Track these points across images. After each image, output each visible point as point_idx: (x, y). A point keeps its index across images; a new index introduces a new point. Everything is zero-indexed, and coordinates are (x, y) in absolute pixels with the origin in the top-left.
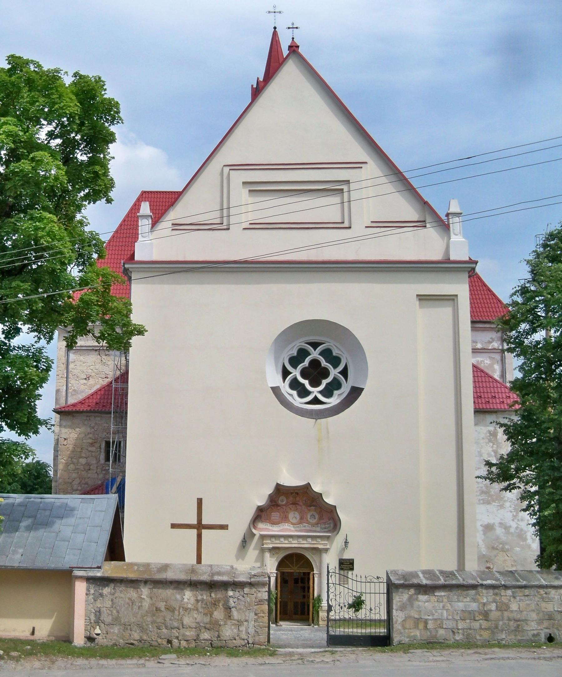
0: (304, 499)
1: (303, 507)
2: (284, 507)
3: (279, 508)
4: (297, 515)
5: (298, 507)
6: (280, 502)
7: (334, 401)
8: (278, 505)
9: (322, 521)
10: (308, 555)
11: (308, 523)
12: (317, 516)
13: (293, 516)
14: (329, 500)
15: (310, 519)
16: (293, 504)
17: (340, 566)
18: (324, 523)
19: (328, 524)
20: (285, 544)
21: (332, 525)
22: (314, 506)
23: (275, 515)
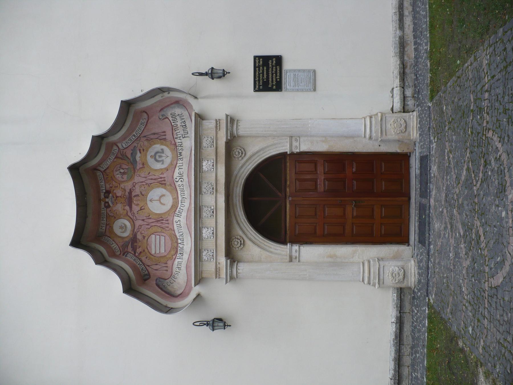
0: (118, 177)
1: (137, 179)
2: (138, 223)
3: (139, 237)
4: (156, 193)
5: (137, 191)
7: (244, 154)
8: (134, 240)
9: (169, 136)
10: (245, 168)
11: (173, 166)
12: (157, 147)
13: (158, 202)
14: (106, 118)
15: (163, 162)
17: (271, 90)
18: (173, 129)
19: (175, 120)
20: (215, 225)
21: (178, 111)
22: (134, 154)
23: (157, 245)
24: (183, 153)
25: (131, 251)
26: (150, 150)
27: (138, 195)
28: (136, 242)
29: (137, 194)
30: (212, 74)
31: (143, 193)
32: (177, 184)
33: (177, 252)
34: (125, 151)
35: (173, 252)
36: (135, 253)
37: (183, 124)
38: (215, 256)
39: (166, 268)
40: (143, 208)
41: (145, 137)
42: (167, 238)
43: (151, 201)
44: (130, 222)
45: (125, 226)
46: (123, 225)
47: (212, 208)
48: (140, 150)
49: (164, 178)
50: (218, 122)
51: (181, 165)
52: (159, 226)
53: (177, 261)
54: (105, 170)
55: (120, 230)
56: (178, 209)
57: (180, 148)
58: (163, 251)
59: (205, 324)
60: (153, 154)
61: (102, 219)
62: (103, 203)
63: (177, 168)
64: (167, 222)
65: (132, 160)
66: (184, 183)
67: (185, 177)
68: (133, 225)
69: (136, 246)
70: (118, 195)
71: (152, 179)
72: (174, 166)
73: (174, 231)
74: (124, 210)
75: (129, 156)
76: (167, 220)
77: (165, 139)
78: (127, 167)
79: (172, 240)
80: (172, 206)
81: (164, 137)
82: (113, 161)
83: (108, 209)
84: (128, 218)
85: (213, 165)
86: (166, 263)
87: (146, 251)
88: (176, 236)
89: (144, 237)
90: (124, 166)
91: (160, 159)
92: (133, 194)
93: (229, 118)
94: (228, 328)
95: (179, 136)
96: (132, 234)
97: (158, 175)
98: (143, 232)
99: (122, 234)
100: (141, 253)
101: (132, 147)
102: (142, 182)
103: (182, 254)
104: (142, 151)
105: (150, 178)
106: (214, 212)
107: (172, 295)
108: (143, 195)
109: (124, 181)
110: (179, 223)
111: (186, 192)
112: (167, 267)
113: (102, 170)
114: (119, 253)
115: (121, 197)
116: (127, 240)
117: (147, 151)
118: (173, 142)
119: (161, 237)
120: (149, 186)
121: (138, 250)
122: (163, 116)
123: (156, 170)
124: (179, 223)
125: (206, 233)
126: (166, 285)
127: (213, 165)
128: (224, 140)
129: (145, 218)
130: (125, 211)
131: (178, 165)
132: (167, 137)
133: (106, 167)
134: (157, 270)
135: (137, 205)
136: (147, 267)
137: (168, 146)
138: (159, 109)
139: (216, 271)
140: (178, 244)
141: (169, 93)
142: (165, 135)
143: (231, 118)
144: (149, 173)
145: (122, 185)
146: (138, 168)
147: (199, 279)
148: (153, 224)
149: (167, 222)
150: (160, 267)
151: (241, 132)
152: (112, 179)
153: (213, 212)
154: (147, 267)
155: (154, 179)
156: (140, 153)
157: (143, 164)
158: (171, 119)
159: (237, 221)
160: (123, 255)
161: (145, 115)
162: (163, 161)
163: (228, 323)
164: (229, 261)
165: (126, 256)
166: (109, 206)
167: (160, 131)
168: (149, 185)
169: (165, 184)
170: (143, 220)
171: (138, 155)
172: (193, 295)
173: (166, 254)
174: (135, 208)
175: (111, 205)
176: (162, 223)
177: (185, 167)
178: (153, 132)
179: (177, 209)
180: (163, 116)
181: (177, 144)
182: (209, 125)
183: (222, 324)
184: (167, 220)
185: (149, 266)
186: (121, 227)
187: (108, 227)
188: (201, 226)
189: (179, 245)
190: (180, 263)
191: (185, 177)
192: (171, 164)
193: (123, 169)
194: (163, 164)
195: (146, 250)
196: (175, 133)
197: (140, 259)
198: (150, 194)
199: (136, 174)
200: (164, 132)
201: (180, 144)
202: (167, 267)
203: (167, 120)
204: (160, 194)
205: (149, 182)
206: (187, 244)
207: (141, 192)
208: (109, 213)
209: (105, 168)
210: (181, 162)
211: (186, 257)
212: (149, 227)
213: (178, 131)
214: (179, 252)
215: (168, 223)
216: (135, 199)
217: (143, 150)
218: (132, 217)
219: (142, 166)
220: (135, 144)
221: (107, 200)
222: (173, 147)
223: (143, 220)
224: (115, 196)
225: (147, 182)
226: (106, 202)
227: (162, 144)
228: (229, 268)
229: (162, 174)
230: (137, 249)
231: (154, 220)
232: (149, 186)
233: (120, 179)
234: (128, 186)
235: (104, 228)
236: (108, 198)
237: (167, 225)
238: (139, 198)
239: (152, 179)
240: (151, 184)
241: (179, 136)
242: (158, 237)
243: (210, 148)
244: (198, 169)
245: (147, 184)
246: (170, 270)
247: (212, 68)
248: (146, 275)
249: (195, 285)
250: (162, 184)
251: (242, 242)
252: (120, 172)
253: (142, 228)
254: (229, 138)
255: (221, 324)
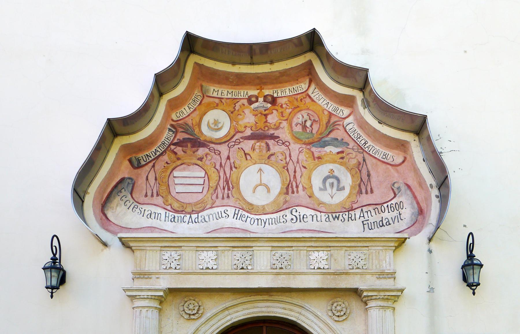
1: (295, 147)
2: (223, 149)
3: (201, 151)
4: (273, 178)
5: (275, 148)
6: (206, 132)
9: (365, 199)
11: (317, 206)
12: (347, 180)
13: (259, 181)
16: (255, 137)
18: (378, 206)
19: (391, 208)
21: (408, 212)
22: (336, 142)
23: (188, 179)
24: (338, 222)
25: (178, 137)
26: (343, 168)
27: (268, 148)
28: (192, 147)
29: (271, 147)
30: (471, 266)
31: (272, 158)
32: (287, 212)
33: (177, 211)
34: (341, 128)
35: (176, 205)
36: (174, 144)
37: (384, 222)
38: (170, 271)
39: (149, 194)
40: (248, 157)
41: (364, 160)
42: (200, 196)
43: (260, 170)
44: (226, 136)
45: (219, 129)
46: (220, 126)
47: (249, 267)
48: (342, 152)
49: (298, 192)
50: (392, 275)
51: (319, 219)
52: (218, 184)
53: (163, 212)
54: (310, 97)
55: (212, 121)
56: (247, 214)
57: (346, 217)
58: (179, 189)
59: (55, 255)
60: (336, 173)
61: (230, 91)
62: (255, 92)
63: (313, 212)
64: (225, 196)
65: (327, 139)
66: (289, 224)
67: (298, 225)
68: (220, 142)
69: (187, 146)
70: (269, 118)
71: (295, 172)
72: (316, 207)
73: (212, 207)
74: (245, 127)
75: (332, 135)
76: (228, 197)
77: (360, 192)
78: (314, 132)
79: (196, 204)
80: (251, 205)
81: (364, 191)
82: (323, 110)
83: (245, 102)
84: (232, 133)
85: (319, 268)
86: (158, 195)
87: (178, 162)
88: (203, 210)
89: (201, 159)
90: (316, 127)
91: (327, 184)
92: (271, 142)
93: (399, 293)
94: (48, 293)
95: (365, 214)
96: (205, 140)
97: (302, 181)
98: (209, 157)
99: (206, 123)
100: (176, 153)
101: (347, 139)
102: (290, 156)
103: (173, 220)
104: (341, 155)
105: (298, 169)
106: (242, 271)
107: (104, 204)
108: (269, 158)
109: (291, 127)
110: (224, 215)
111: (274, 226)
112: (152, 196)
113: (310, 92)
114: (175, 118)
115: (266, 122)
116: (197, 130)
117: (341, 164)
118: (355, 206)
119: (202, 187)
120: (284, 168)
121: (179, 150)
122: (398, 188)
123: (310, 178)
124: (224, 215)
125: (207, 258)
126: (122, 195)
127: (319, 268)
128: (361, 286)
129: (232, 161)
130: (243, 129)
131: (319, 214)
132: (364, 195)
133: (314, 99)
134: (147, 179)
135: (253, 149)
136: (151, 164)
137: (349, 197)
138: (410, 183)
139: (145, 274)
140: (190, 214)
141: (437, 197)
142: (367, 193)
143: (398, 296)
144: (305, 168)
145: (285, 124)
146: (314, 149)
147: (131, 244)
148: (222, 174)
149: (225, 196)
150: (152, 185)
151: (374, 314)
152: (295, 108)
153: (242, 268)
154: (151, 164)
155: (295, 176)
156: (338, 153)
157: (319, 158)
158: (393, 202)
159: (227, 309)
160: (172, 125)
161: (399, 160)
162: (325, 189)
163: (56, 293)
164: (161, 294)
165: (170, 130)
166: (250, 102)
167: (374, 185)
168: (286, 167)
169: (287, 193)
170: (228, 158)
171: (335, 150)
172: (105, 236)
173: (173, 193)
174: (247, 145)
175: (253, 106)
176: (224, 189)
177: (314, 225)
178: (372, 172)
179: (247, 212)
180: (398, 188)
181: (352, 213)
182: (386, 260)
183: (54, 283)
184: (228, 197)
185: (154, 166)
186: (216, 122)
187: (217, 101)
188: (220, 248)
189: (188, 216)
190: (157, 216)
191: (298, 225)
192: (321, 203)
193: (311, 126)
194: (321, 189)
195: (179, 163)
196: (371, 208)
197: (165, 151)
198: (271, 168)
199: (304, 146)
200: (372, 192)
201: (353, 218)
202: (152, 196)
203: (392, 195)
204: (270, 185)
205: (291, 167)
206: (190, 229)
207: (272, 155)
208: (240, 103)
209: (312, 96)
210: (324, 218)
211: (169, 226)
212: (218, 167)
213: (373, 213)
214: (176, 215)
215: (223, 198)
216: (263, 144)
217: (342, 158)
218: (234, 140)
219: (316, 155)
220: (352, 144)
221: (261, 99)
222: (347, 206)
223: (228, 158)
224: (267, 112)
225: (291, 163)
226: (257, 98)
227: (352, 188)
228: (150, 293)
229: (304, 189)
230: (181, 148)
231: (228, 176)
232: (284, 168)
233: (295, 121)
234: (284, 134)
235: (215, 95)
236: (265, 101)
237: (220, 196)
238: (264, 151)
239: (295, 172)
240: (287, 170)
241: (365, 214)
242: (201, 181)
243: (347, 263)
244: (313, 244)
245: (287, 163)
246: (146, 200)
247: (481, 266)
248: (139, 161)
249: (120, 239)
250: (287, 188)
251: (192, 317)
252: (306, 121)
253: (215, 156)
254: (365, 294)
255: (54, 283)
